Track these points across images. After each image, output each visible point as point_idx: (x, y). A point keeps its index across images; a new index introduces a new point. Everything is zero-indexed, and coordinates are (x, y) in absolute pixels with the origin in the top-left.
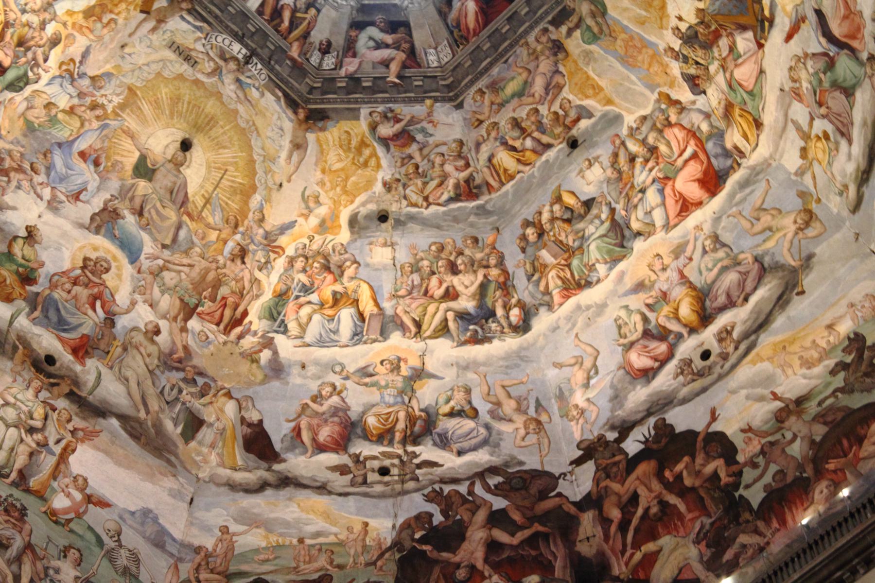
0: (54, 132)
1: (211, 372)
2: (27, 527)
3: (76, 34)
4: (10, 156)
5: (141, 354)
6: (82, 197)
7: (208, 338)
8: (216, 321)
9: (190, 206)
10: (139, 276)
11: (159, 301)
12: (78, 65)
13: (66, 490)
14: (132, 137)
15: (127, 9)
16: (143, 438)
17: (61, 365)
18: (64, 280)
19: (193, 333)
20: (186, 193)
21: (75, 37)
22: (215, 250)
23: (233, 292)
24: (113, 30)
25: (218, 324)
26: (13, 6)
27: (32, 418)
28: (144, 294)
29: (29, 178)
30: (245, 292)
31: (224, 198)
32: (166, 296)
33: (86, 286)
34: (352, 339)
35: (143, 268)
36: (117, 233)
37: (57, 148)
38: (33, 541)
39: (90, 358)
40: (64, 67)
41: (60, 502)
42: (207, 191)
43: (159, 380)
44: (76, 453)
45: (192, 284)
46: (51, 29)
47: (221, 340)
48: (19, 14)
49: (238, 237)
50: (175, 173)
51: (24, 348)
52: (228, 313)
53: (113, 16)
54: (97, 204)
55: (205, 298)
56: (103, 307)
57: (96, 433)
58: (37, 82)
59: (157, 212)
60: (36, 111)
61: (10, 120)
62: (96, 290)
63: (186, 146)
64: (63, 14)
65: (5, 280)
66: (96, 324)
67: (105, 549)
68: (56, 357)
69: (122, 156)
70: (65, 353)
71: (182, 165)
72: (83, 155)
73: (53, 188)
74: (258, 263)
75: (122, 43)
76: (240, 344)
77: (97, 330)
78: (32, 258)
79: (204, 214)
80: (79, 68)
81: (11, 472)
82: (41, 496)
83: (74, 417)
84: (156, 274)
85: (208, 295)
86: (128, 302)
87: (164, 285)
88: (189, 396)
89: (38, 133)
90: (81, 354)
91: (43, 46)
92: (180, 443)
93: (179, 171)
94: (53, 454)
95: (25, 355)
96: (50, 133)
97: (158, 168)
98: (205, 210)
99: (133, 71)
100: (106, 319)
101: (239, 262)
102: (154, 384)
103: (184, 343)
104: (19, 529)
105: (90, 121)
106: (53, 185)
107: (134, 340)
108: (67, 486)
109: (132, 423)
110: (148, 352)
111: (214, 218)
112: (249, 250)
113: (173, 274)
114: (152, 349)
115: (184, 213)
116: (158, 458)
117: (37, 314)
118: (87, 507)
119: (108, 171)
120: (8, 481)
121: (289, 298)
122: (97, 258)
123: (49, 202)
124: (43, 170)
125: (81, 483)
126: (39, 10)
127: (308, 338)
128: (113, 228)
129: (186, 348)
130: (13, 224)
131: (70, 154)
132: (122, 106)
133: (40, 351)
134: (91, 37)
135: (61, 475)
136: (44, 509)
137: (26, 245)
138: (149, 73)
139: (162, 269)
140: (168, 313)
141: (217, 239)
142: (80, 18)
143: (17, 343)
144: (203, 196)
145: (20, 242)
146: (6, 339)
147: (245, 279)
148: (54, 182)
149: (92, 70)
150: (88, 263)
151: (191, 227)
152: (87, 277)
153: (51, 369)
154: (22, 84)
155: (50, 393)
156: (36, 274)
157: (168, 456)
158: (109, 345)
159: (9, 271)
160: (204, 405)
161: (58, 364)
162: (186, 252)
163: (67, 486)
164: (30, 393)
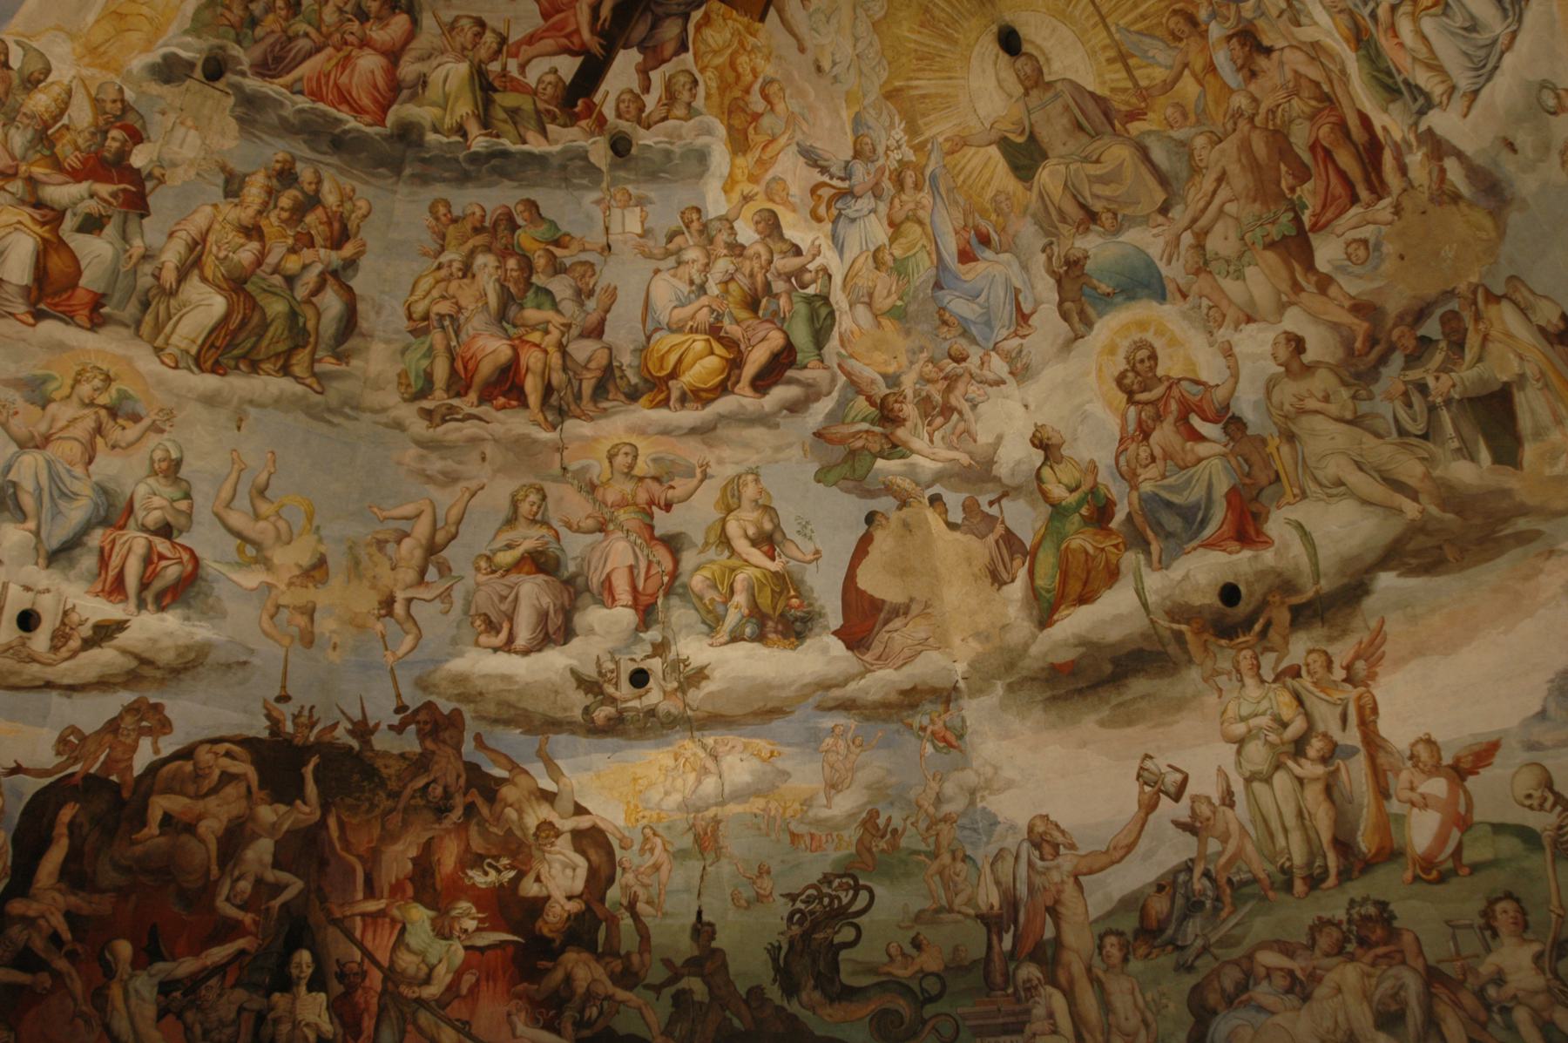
0: (917, 280)
1: (1431, 290)
2: (1407, 938)
3: (768, 176)
4: (929, 381)
5: (1317, 412)
6: (1026, 309)
7: (1365, 242)
8: (1345, 200)
9: (1119, 103)
10: (1190, 299)
11: (1251, 296)
12: (826, 179)
13: (1415, 797)
14: (965, 143)
15: (749, 53)
16: (1450, 552)
17: (1248, 584)
18: (1132, 447)
19: (1341, 269)
20: (1092, 94)
21: (774, 179)
22: (1217, 103)
23: (1312, 117)
24: (782, 89)
25: (1354, 199)
26: (689, 310)
27: (1285, 725)
28: (1224, 316)
29: (966, 378)
30: (1326, 88)
31: (1131, 16)
32: (1250, 271)
33: (1159, 418)
34: (1504, 10)
35: (1181, 282)
36: (1104, 288)
37: (940, 293)
38: (1431, 961)
39: (1267, 519)
40: (822, 210)
41: (1422, 831)
42: (1105, 48)
43: (1377, 416)
44: (1381, 710)
45: (1255, 200)
46: (747, 233)
47: (1387, 215)
48: (704, 300)
49: (1216, 31)
50: (1050, 94)
51: (1188, 622)
52: (1345, 159)
53: (757, 87)
54: (1046, 288)
55: (1293, 190)
56: (1205, 419)
57: (1378, 636)
58: (830, 277)
59: (1103, 180)
60: (879, 287)
61: (876, 348)
62: (1174, 406)
63: (1010, 42)
64: (728, 201)
65: (1087, 553)
66: (1224, 455)
67: (1546, 842)
68: (1231, 580)
69: (988, 183)
70: (1235, 557)
71: (1040, 72)
72: (966, 256)
73: (994, 349)
74: (1285, 17)
75: (813, 69)
76: (1416, 184)
77: (1233, 462)
78: (1077, 475)
79: (1143, 83)
80: (832, 178)
81: (1325, 857)
82: (1391, 854)
83: (1331, 650)
84: (1203, 265)
85: (1290, 180)
86: (1221, 362)
87: (1228, 262)
88: (1444, 377)
89: (912, 308)
90: (1252, 532)
91: (771, 253)
92: (1509, 480)
93: (1050, 85)
94: (1351, 752)
95: (1197, 633)
96: (916, 288)
97: (1031, 125)
98: (1137, 73)
99: (861, 73)
100: (1225, 428)
101: (1262, 62)
102: (1378, 435)
103: (1347, 304)
104: (1398, 957)
105: (918, 203)
106: (991, 345)
107: (1287, 407)
108: (1412, 789)
109: (1411, 546)
110: (1320, 395)
111: (1156, 65)
112: (1250, 22)
113: (1219, 228)
114: (1322, 381)
115: (1124, 125)
116: (1500, 553)
117: (1155, 548)
118: (1466, 792)
119: (1003, 229)
120: (1332, 881)
121: (1367, 30)
122: (1127, 358)
123: (1011, 373)
124: (962, 344)
125: (1428, 750)
126: (708, 255)
127: (1464, 82)
128: (1095, 288)
129: (1360, 308)
130: (1019, 463)
131: (957, 278)
132: (912, 130)
133: (1207, 601)
134: (783, 140)
135: (1390, 774)
136: (1409, 875)
137: (1056, 467)
138: (871, 44)
139: (1200, 246)
140: (1279, 293)
141: (1200, 83)
142: (745, 162)
143: (1175, 626)
144: (1110, 61)
145: (1046, 472)
146: (1160, 639)
147: (1303, 69)
148: (987, 339)
149: (839, 150)
150: (1127, 381)
151: (1154, 128)
152: (1146, 403)
153: (1243, 609)
154: (824, 312)
155: (1272, 650)
156: (1102, 490)
157: (1509, 531)
158: (1267, 461)
159: (1076, 532)
160: (1480, 359)
161: (1243, 589)
162: (1195, 170)
163: (1412, 789)
164: (1252, 689)
